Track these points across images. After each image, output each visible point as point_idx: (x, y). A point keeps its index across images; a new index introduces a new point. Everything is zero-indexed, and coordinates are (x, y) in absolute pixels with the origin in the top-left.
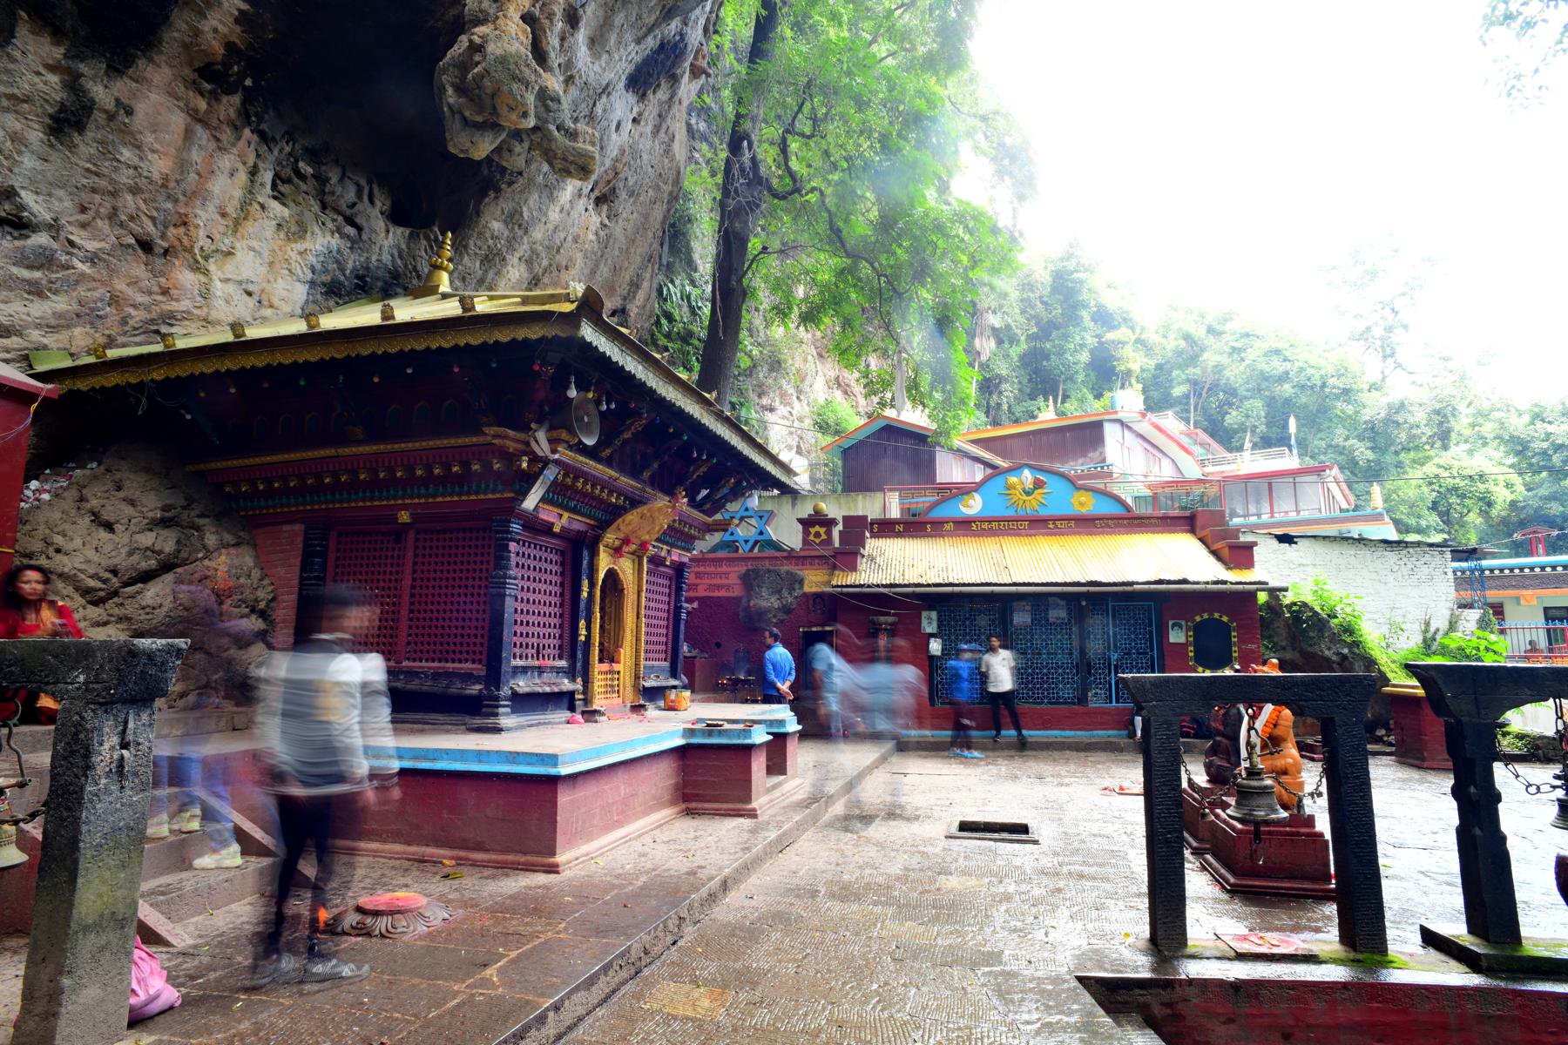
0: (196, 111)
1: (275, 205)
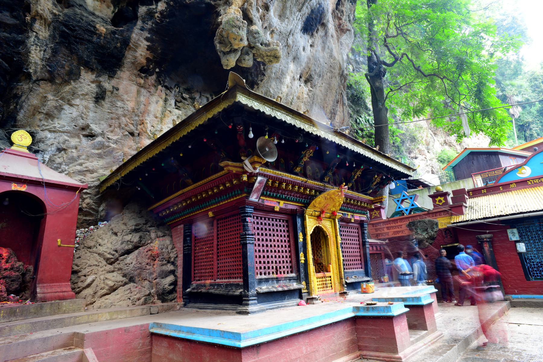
0: (140, 84)
1: (177, 111)
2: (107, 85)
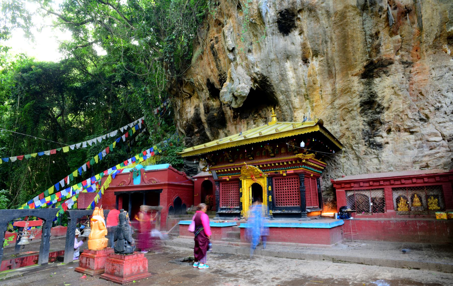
2: (226, 132)
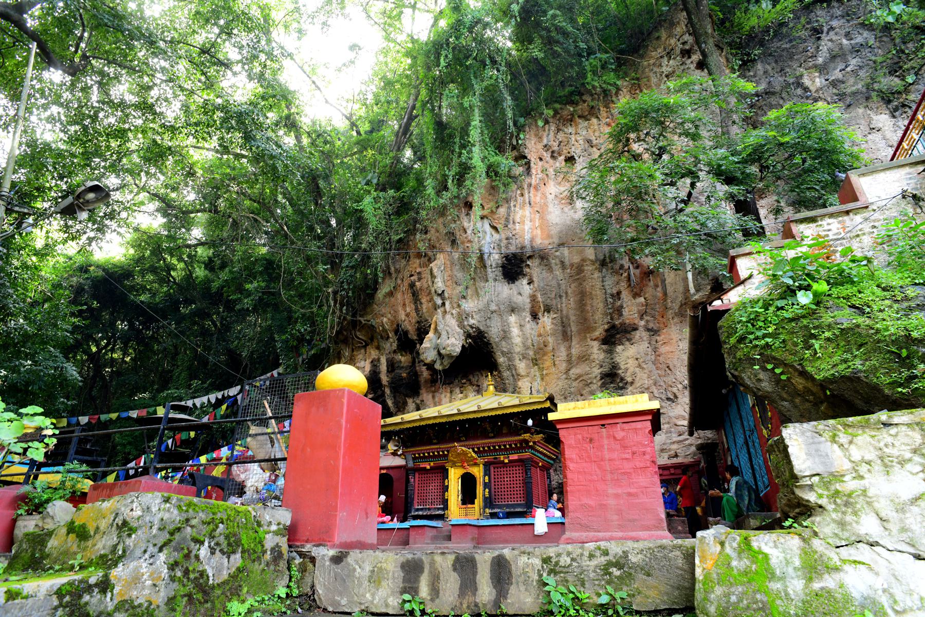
2: (418, 402)
